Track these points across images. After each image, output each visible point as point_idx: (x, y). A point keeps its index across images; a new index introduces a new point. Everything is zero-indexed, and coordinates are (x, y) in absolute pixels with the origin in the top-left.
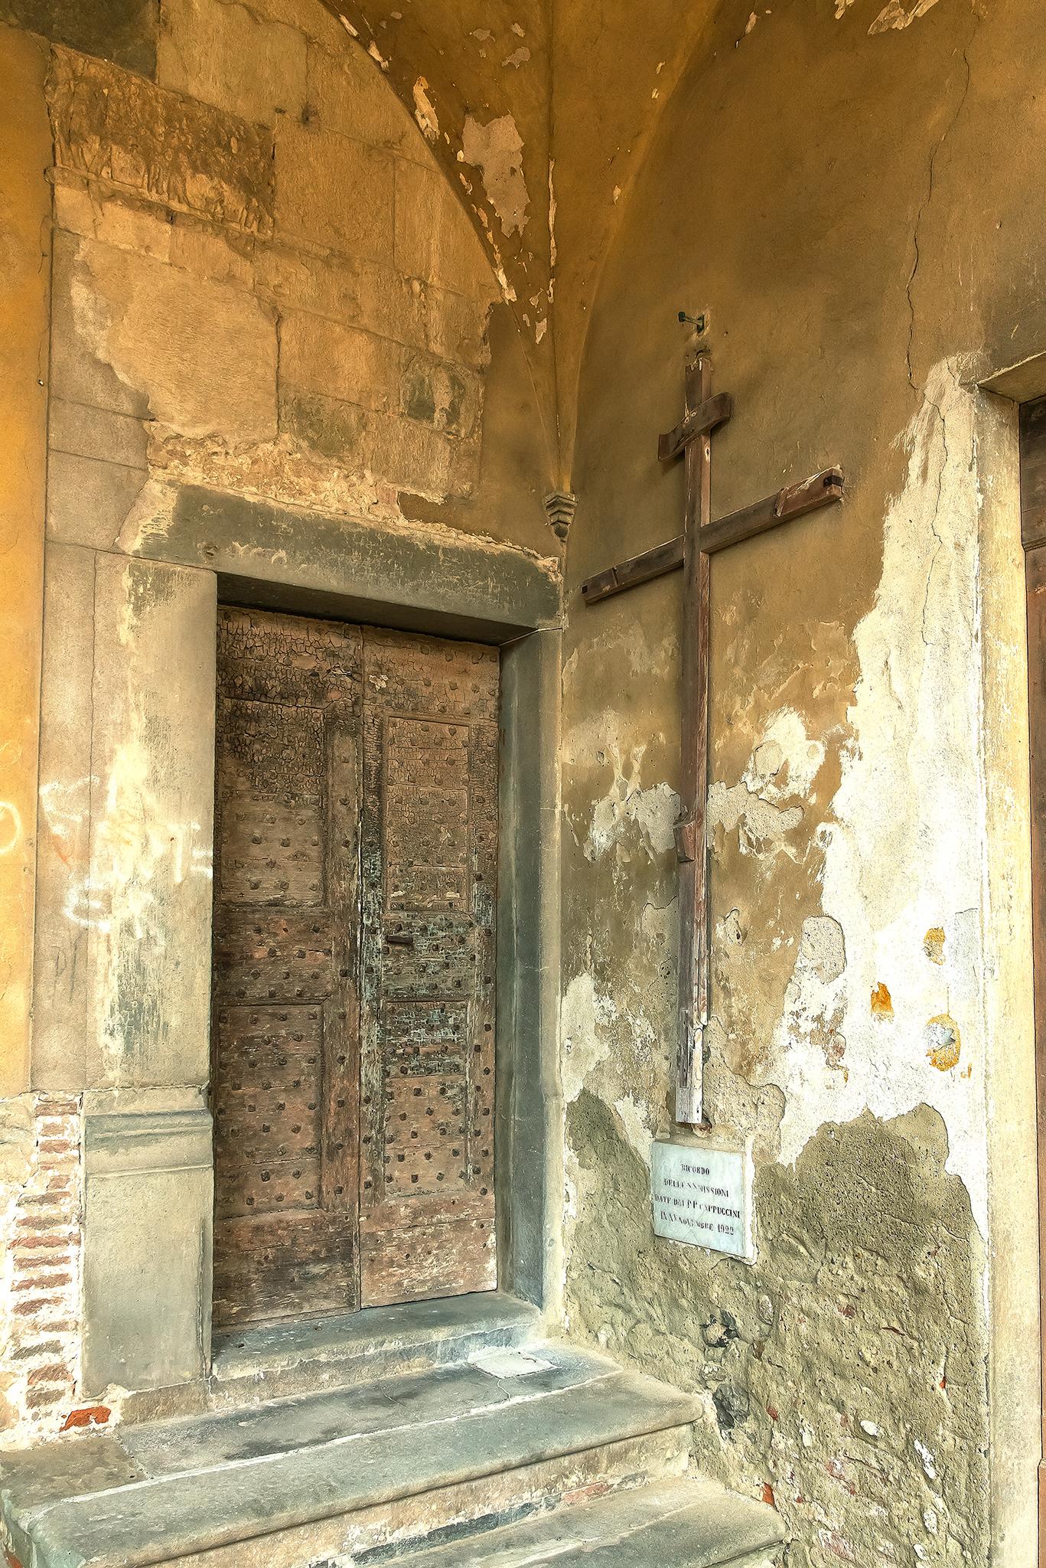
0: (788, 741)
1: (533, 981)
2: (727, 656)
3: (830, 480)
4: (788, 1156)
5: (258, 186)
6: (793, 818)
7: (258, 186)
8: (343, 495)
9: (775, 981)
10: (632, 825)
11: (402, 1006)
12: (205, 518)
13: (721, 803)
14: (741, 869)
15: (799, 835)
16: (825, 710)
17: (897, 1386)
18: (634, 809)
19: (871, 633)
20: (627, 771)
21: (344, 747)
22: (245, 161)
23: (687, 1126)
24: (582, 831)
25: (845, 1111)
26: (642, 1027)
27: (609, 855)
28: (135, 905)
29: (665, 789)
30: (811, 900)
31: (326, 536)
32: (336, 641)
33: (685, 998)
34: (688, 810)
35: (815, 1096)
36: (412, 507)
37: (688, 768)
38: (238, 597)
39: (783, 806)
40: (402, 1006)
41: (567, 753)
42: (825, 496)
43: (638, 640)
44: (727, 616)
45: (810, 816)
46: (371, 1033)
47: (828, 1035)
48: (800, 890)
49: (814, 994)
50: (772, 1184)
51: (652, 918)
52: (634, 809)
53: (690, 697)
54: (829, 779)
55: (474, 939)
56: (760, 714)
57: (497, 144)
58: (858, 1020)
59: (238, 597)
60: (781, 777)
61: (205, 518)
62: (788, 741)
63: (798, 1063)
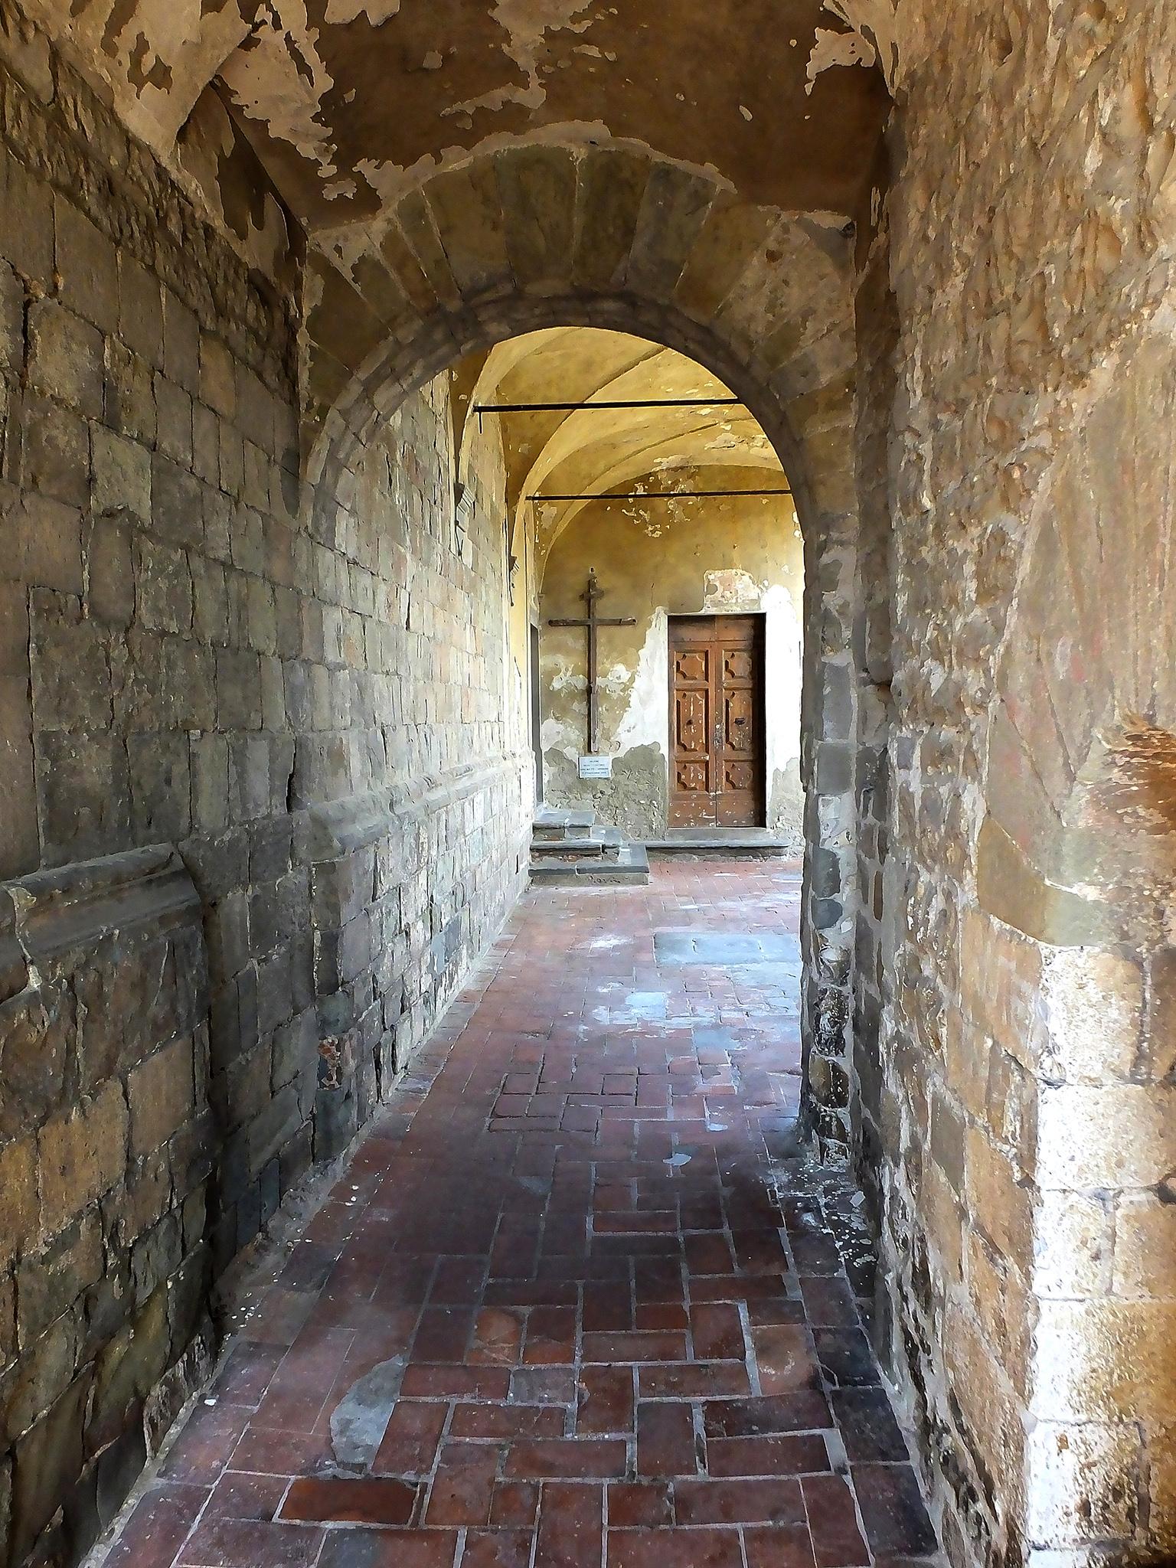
2: (601, 650)
9: (618, 720)
14: (607, 697)
16: (632, 664)
17: (648, 793)
20: (567, 670)
27: (560, 690)
43: (574, 639)
45: (627, 687)
48: (625, 703)
54: (632, 679)
56: (612, 664)
60: (619, 678)
62: (621, 671)
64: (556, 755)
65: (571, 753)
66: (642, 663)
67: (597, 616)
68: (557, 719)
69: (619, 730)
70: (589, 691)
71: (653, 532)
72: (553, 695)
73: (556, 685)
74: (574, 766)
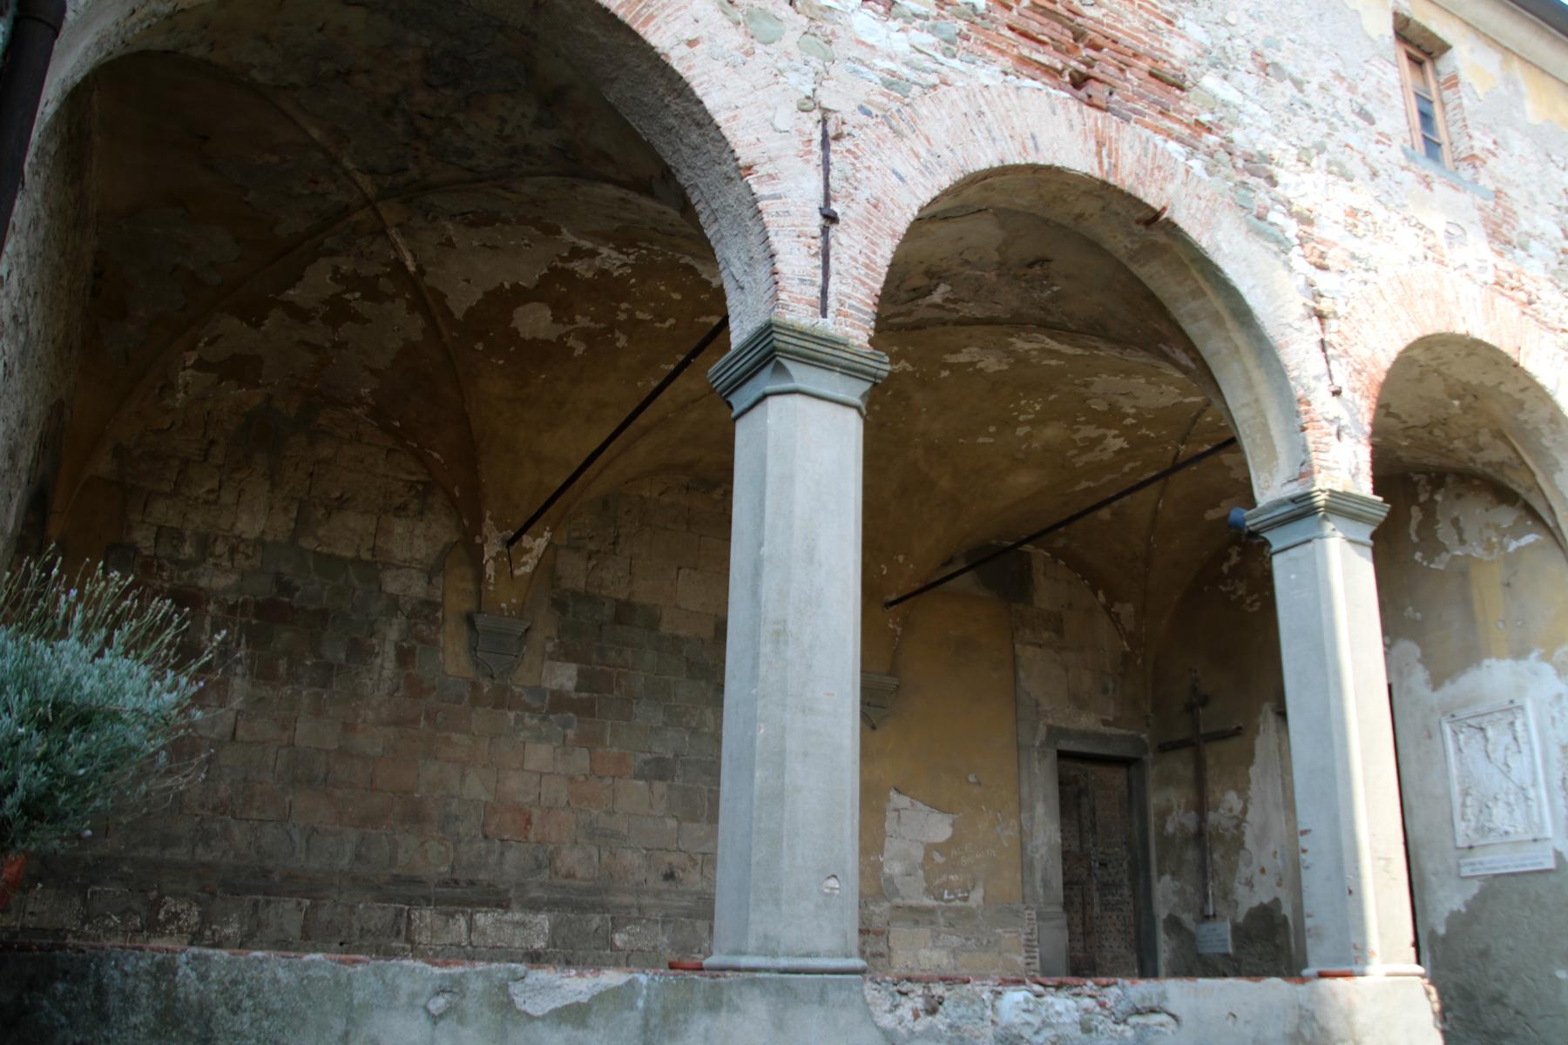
0: (1232, 799)
1: (1148, 879)
3: (1239, 728)
4: (1240, 919)
5: (1059, 631)
6: (1235, 822)
7: (1059, 631)
8: (1087, 721)
9: (1233, 869)
10: (1182, 825)
11: (1105, 887)
12: (1055, 733)
13: (1212, 817)
15: (1238, 826)
16: (1242, 791)
18: (1181, 819)
19: (1254, 771)
21: (1084, 800)
22: (1055, 622)
23: (1207, 917)
24: (1163, 827)
25: (1255, 903)
26: (1189, 889)
28: (1043, 850)
29: (1193, 813)
30: (1241, 845)
31: (1084, 735)
32: (1080, 765)
33: (1205, 877)
34: (1202, 818)
35: (1249, 899)
36: (1105, 723)
37: (1201, 806)
38: (1062, 755)
39: (1232, 818)
40: (1105, 887)
41: (1155, 800)
42: (1238, 732)
44: (1211, 761)
45: (1240, 822)
46: (1096, 895)
47: (1250, 884)
48: (1238, 843)
49: (1243, 872)
50: (1236, 929)
51: (1191, 854)
52: (1181, 819)
53: (1200, 784)
54: (1245, 811)
55: (1125, 865)
57: (1126, 610)
58: (1257, 877)
59: (1062, 755)
60: (1231, 810)
61: (1055, 733)
62: (1232, 799)
63: (1241, 891)
64: (1174, 924)
65: (1187, 919)
66: (1253, 786)
67: (1202, 730)
68: (1173, 874)
69: (1236, 885)
70: (1200, 837)
71: (1251, 605)
72: (1165, 841)
73: (1170, 828)
74: (1192, 938)
